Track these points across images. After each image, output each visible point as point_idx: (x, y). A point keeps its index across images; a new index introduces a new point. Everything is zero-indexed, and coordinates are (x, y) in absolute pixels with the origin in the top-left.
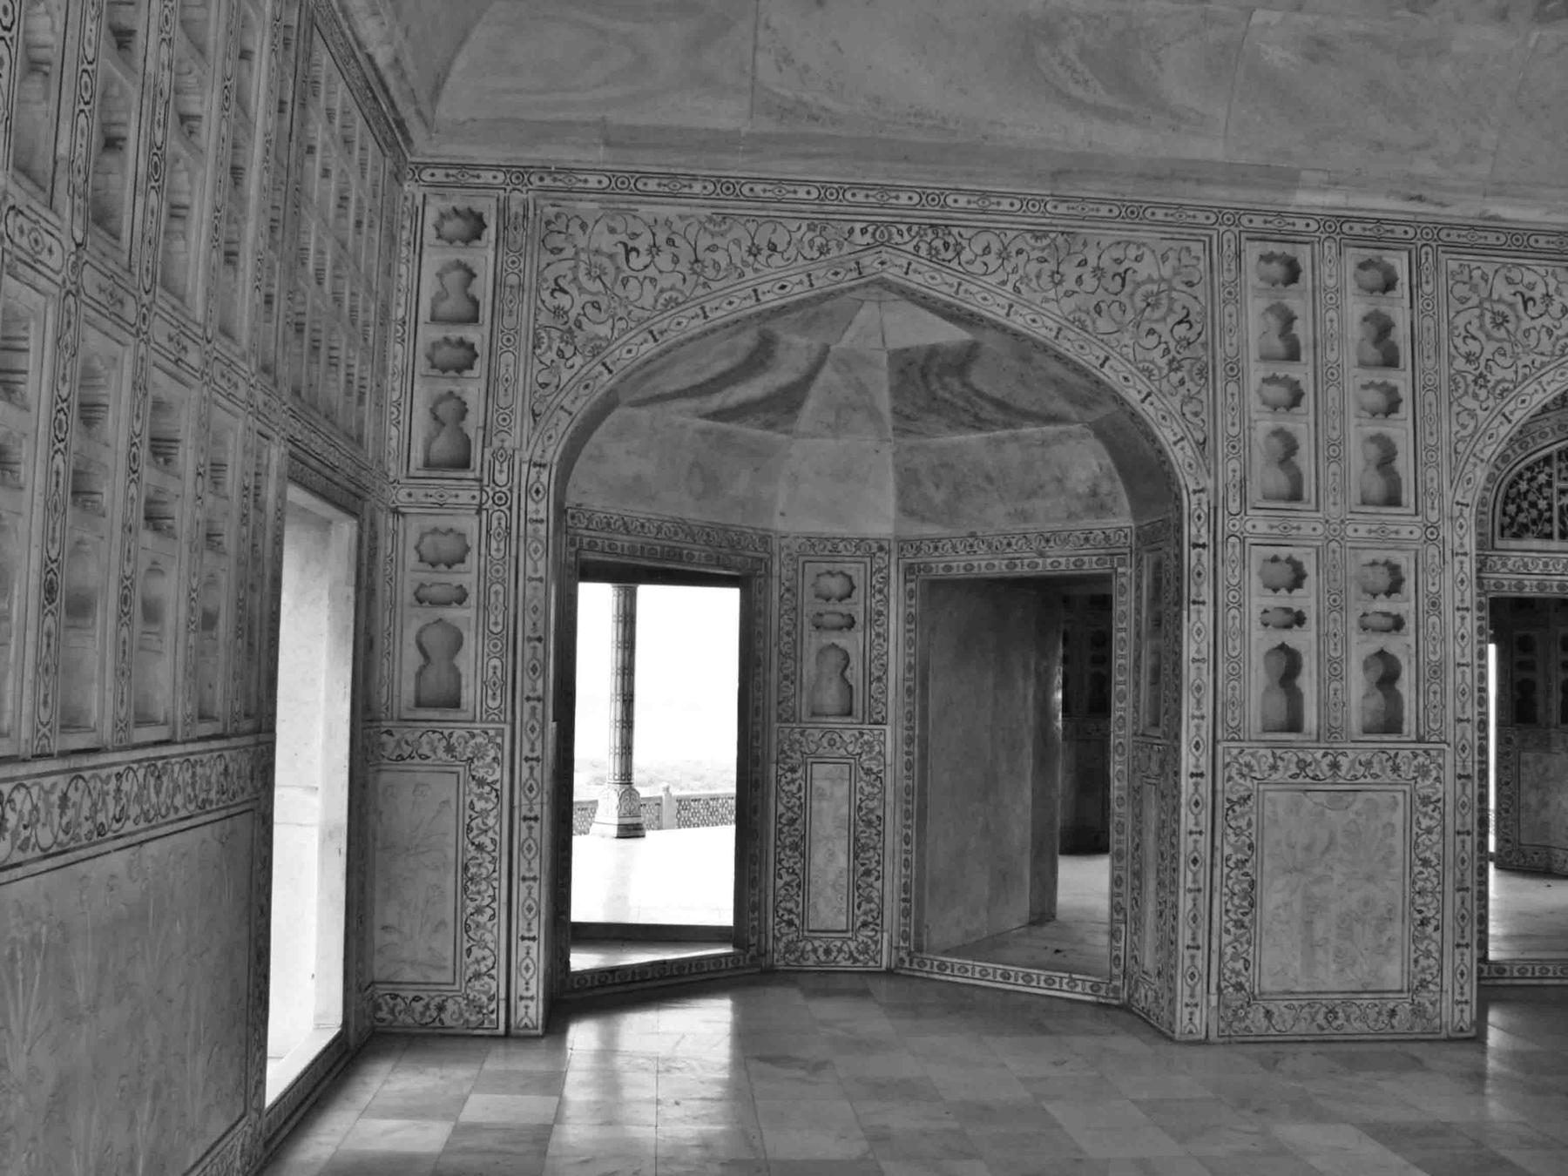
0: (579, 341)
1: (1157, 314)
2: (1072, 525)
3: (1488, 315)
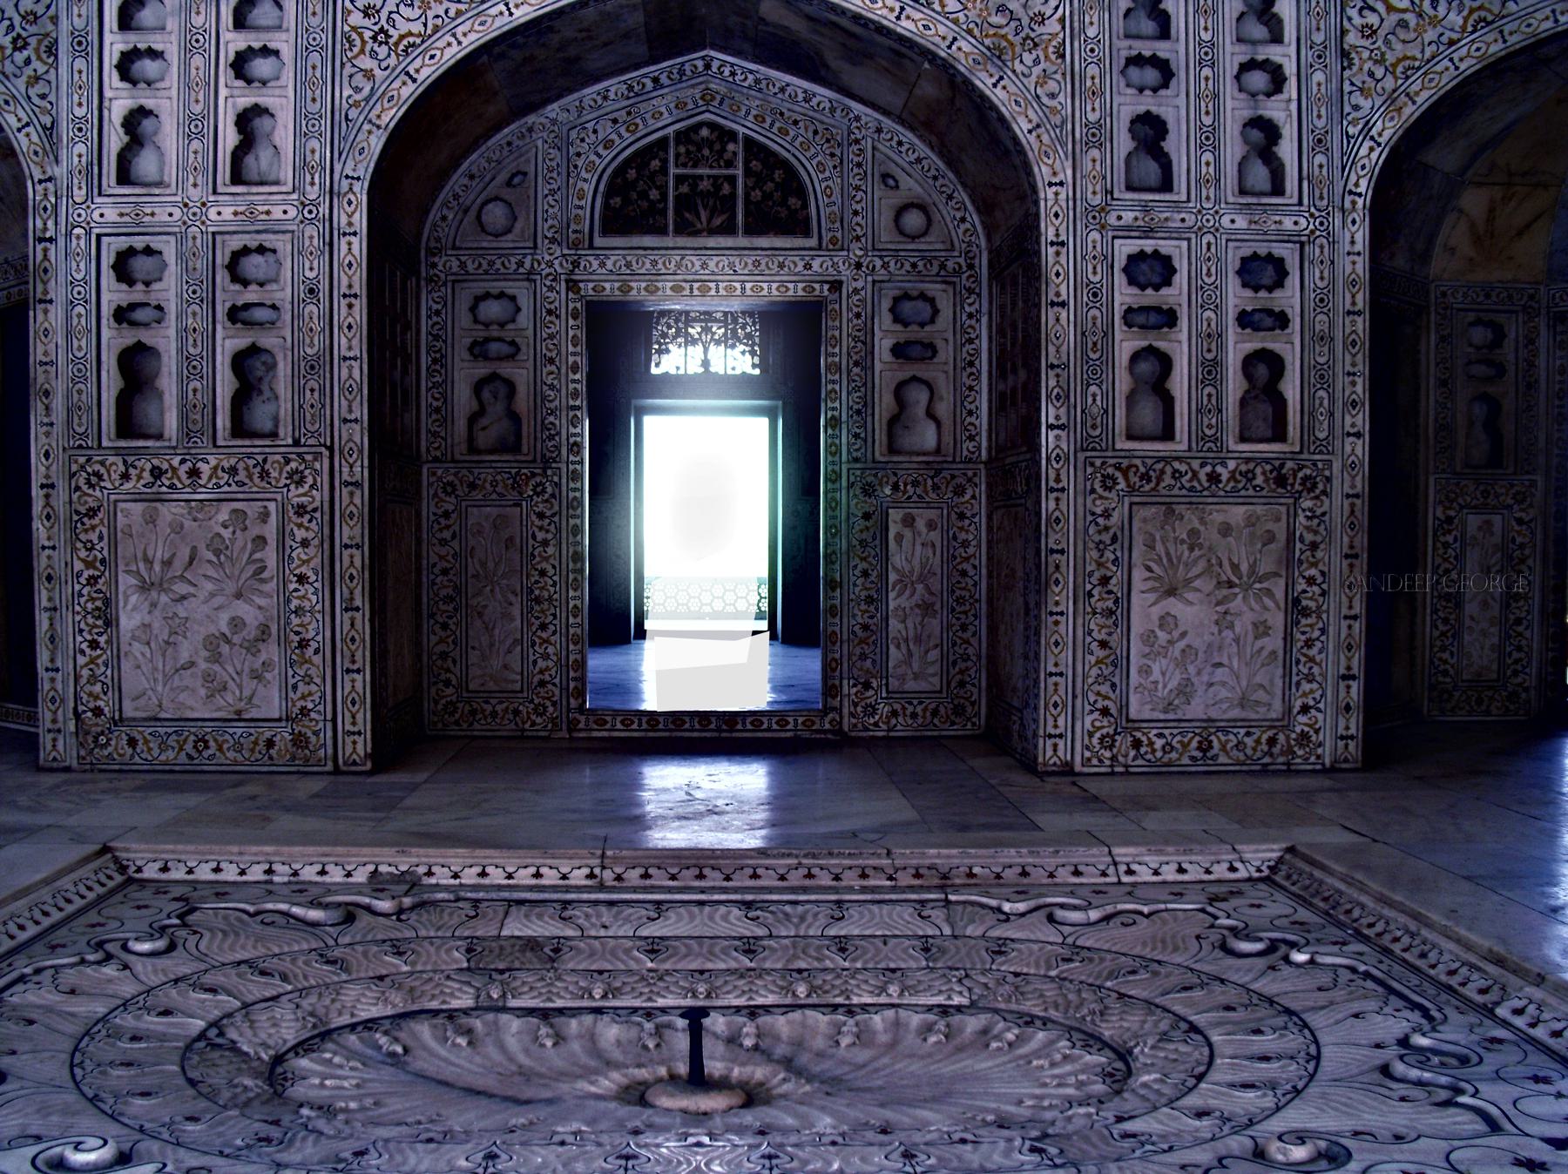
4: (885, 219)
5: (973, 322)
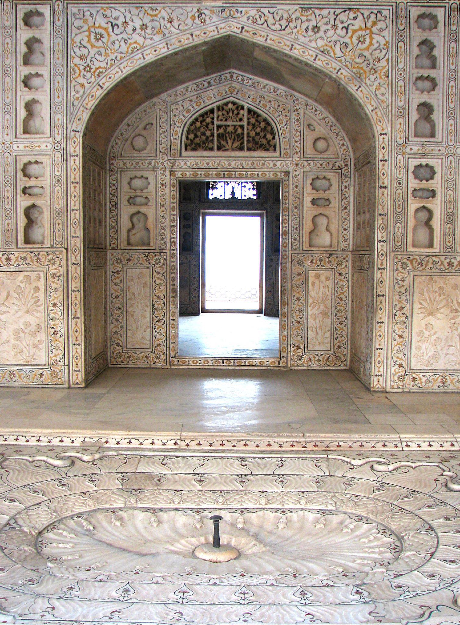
3: (93, 35)
4: (309, 145)
5: (347, 190)
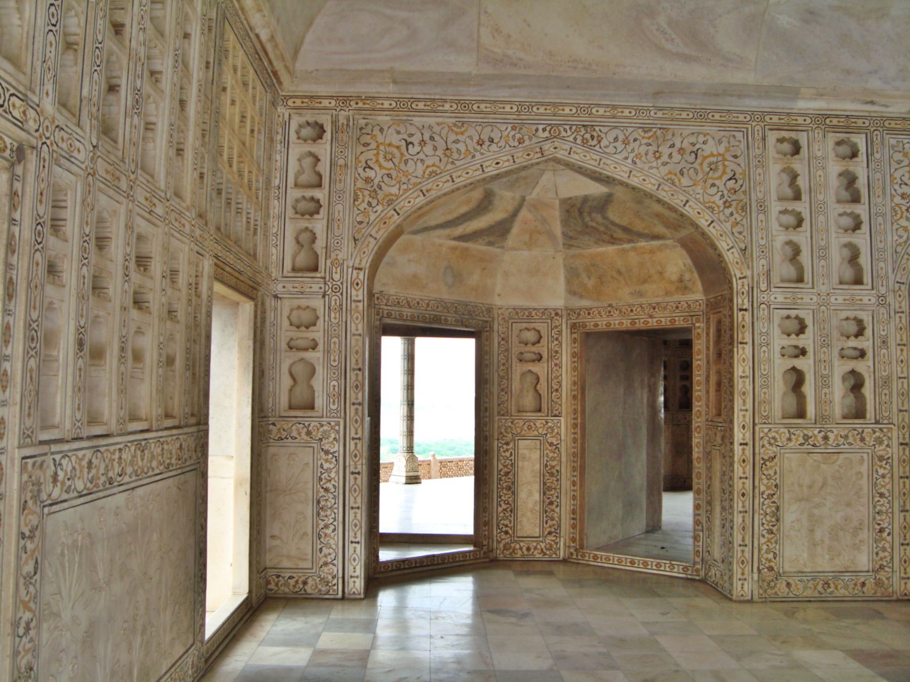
0: (380, 197)
1: (717, 175)
2: (668, 299)
